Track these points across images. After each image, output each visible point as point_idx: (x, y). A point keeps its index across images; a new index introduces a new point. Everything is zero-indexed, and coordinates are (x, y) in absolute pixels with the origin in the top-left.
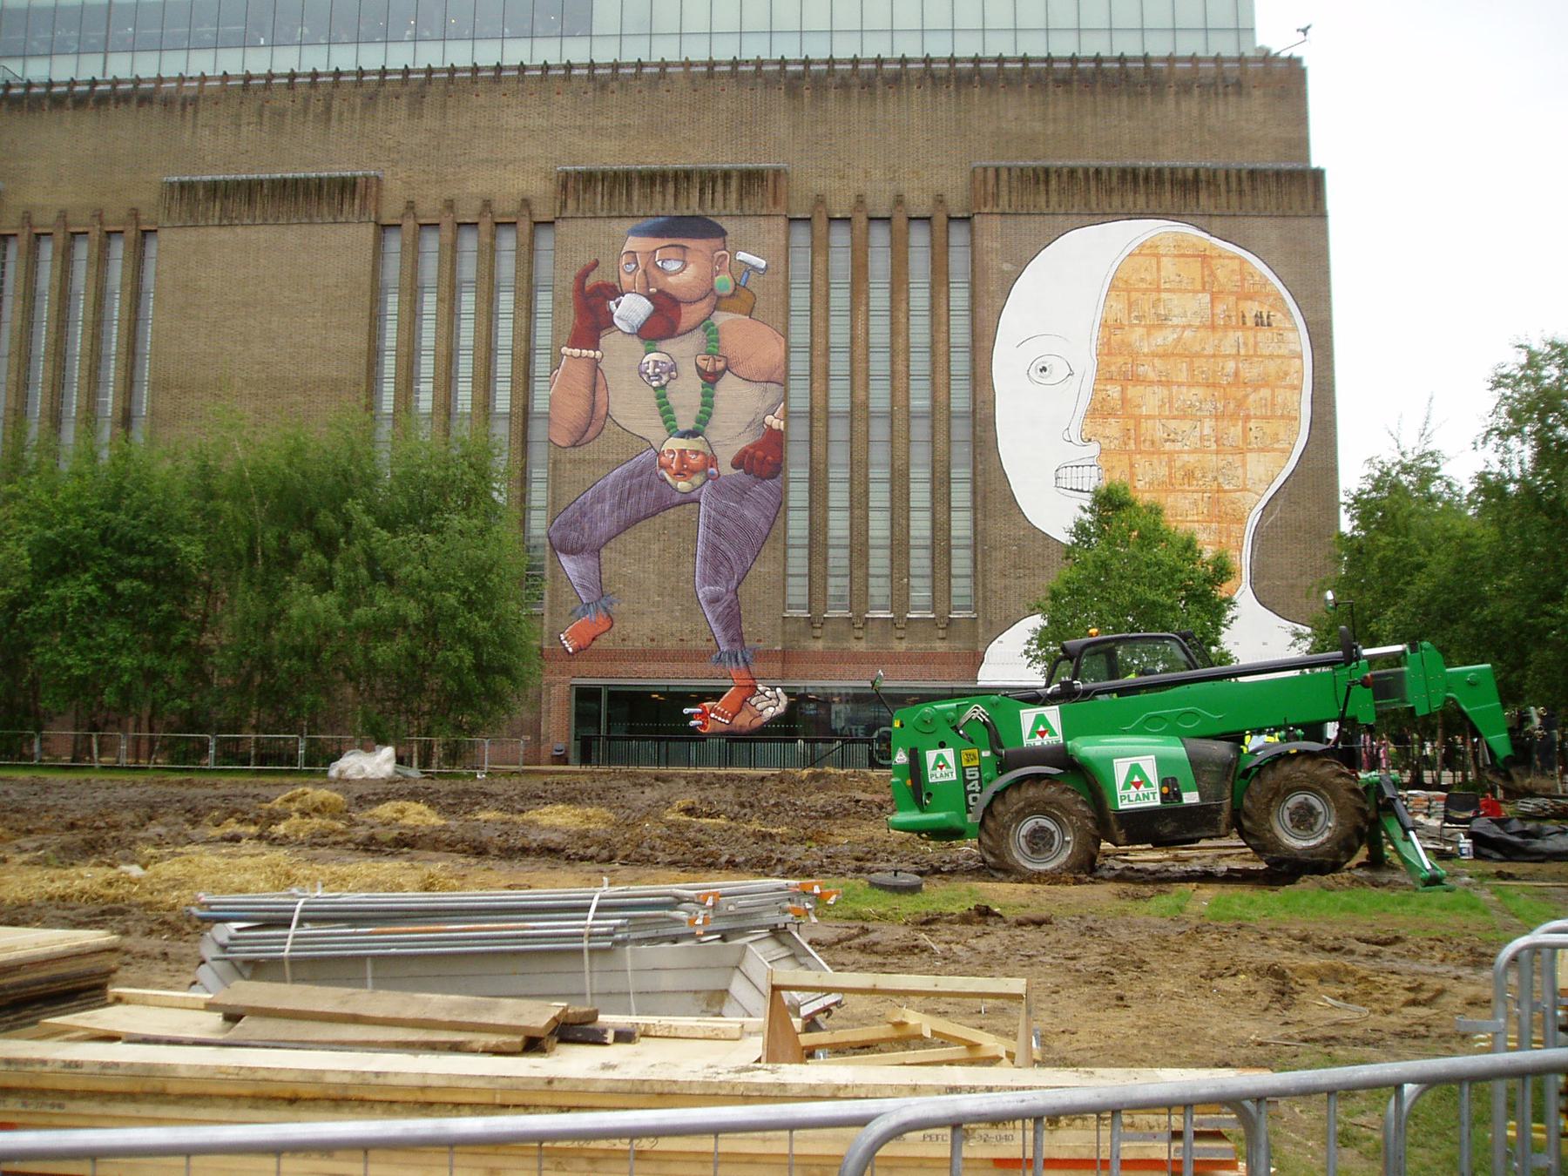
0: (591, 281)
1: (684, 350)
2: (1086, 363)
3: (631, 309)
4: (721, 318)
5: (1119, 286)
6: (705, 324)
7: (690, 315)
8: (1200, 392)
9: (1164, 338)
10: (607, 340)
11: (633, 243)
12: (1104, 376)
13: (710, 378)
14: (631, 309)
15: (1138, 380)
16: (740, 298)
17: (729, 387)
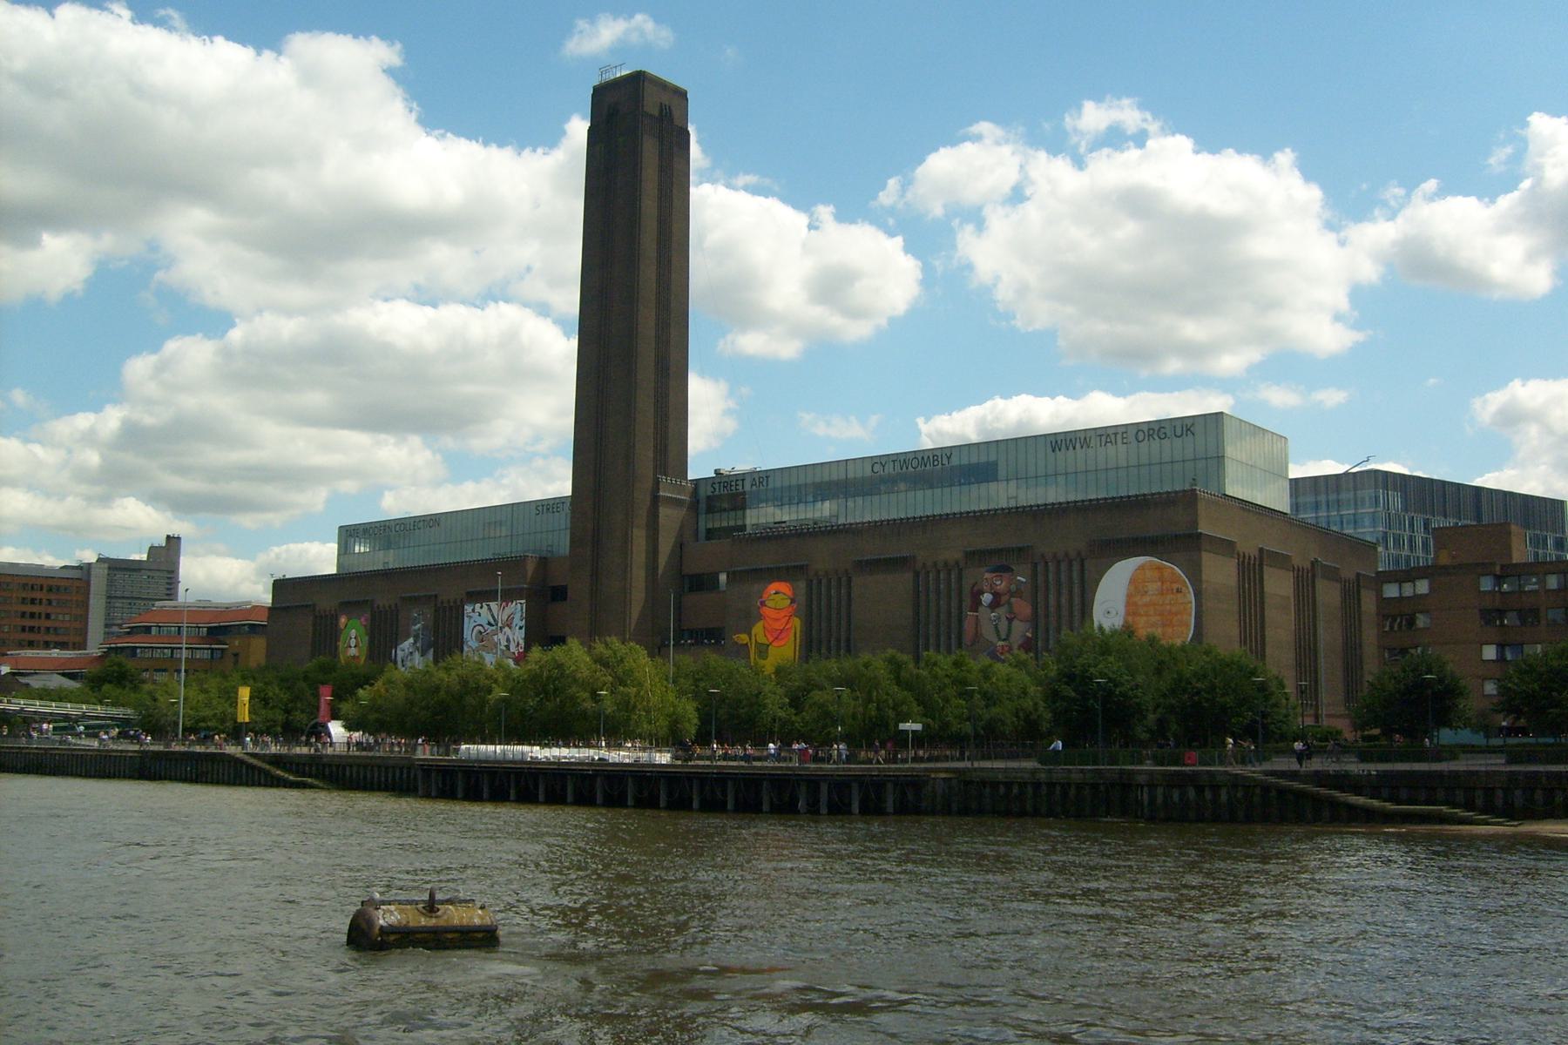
0: (975, 588)
1: (1002, 611)
2: (1122, 609)
3: (987, 598)
4: (1013, 600)
5: (1132, 581)
6: (1009, 603)
7: (1004, 599)
8: (1158, 618)
9: (1147, 599)
10: (980, 609)
11: (987, 575)
12: (1128, 614)
13: (1010, 620)
14: (987, 598)
15: (1140, 615)
16: (1017, 593)
17: (1016, 623)
